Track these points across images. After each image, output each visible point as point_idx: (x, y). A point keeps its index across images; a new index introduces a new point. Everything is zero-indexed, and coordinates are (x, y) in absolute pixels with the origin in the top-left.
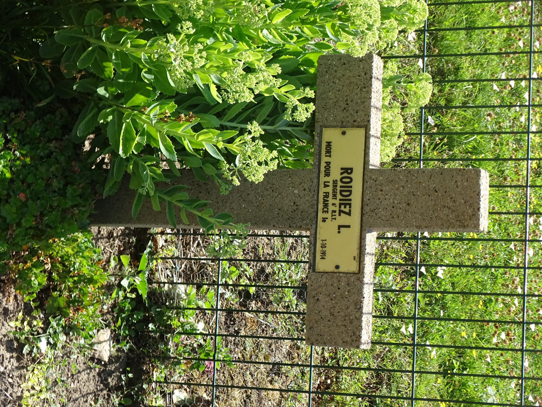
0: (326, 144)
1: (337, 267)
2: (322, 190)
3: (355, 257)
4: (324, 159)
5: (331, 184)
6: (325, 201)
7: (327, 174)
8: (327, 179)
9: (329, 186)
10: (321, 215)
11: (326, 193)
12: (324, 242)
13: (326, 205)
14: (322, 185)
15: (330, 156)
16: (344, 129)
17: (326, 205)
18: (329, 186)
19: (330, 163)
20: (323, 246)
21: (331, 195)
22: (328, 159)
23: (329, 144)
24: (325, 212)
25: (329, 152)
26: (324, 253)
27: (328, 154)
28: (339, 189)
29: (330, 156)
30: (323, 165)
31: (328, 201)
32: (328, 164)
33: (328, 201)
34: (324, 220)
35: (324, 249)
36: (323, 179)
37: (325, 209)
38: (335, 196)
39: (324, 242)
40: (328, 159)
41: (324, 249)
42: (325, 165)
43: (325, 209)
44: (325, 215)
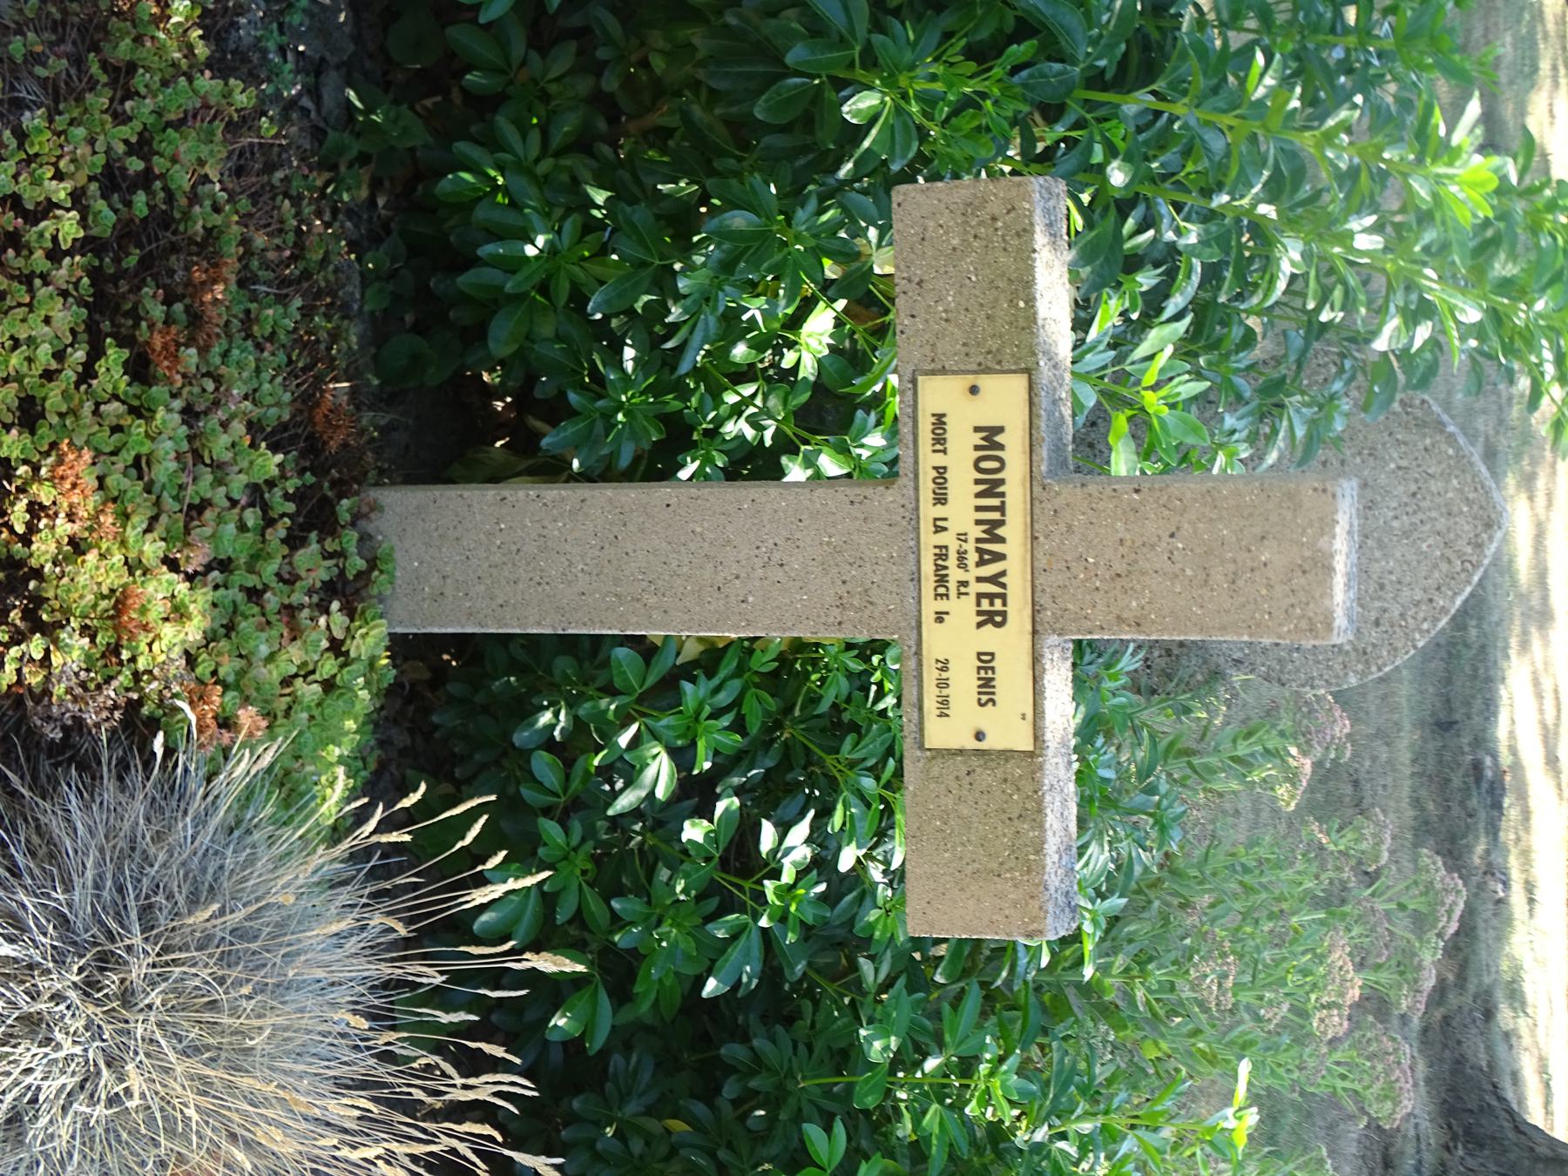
0: (933, 420)
1: (979, 736)
2: (929, 539)
4: (929, 459)
6: (938, 568)
7: (941, 500)
8: (940, 511)
9: (945, 529)
10: (930, 606)
11: (940, 547)
12: (944, 675)
13: (942, 580)
14: (926, 527)
15: (944, 451)
17: (942, 580)
18: (945, 529)
19: (945, 468)
20: (943, 684)
21: (953, 556)
22: (939, 460)
23: (940, 420)
24: (941, 595)
25: (940, 440)
26: (944, 702)
27: (938, 447)
29: (944, 451)
31: (946, 568)
32: (941, 471)
33: (946, 568)
34: (940, 617)
35: (945, 692)
36: (929, 511)
37: (942, 590)
39: (944, 675)
40: (939, 460)
43: (942, 590)
44: (942, 605)
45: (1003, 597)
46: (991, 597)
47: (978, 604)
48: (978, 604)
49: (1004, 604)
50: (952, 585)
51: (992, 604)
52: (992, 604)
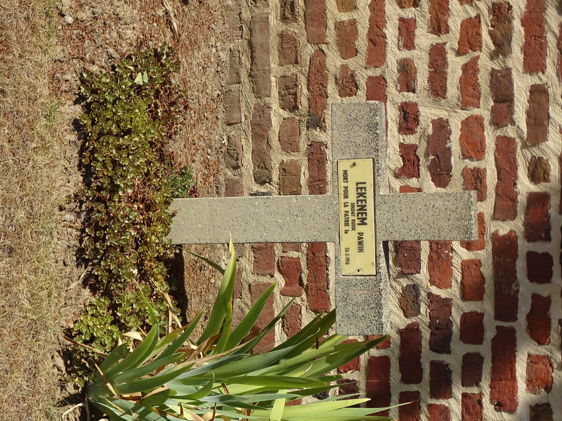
3: (373, 263)
4: (342, 184)
5: (350, 205)
7: (346, 197)
11: (345, 212)
15: (347, 182)
16: (356, 161)
17: (347, 221)
22: (346, 184)
23: (345, 172)
28: (356, 208)
29: (347, 182)
30: (342, 190)
32: (346, 188)
35: (348, 256)
38: (352, 213)
40: (346, 184)
41: (348, 256)
42: (344, 189)
45: (365, 201)
46: (362, 201)
47: (358, 203)
48: (358, 203)
49: (366, 203)
50: (350, 222)
51: (362, 203)
52: (362, 203)
